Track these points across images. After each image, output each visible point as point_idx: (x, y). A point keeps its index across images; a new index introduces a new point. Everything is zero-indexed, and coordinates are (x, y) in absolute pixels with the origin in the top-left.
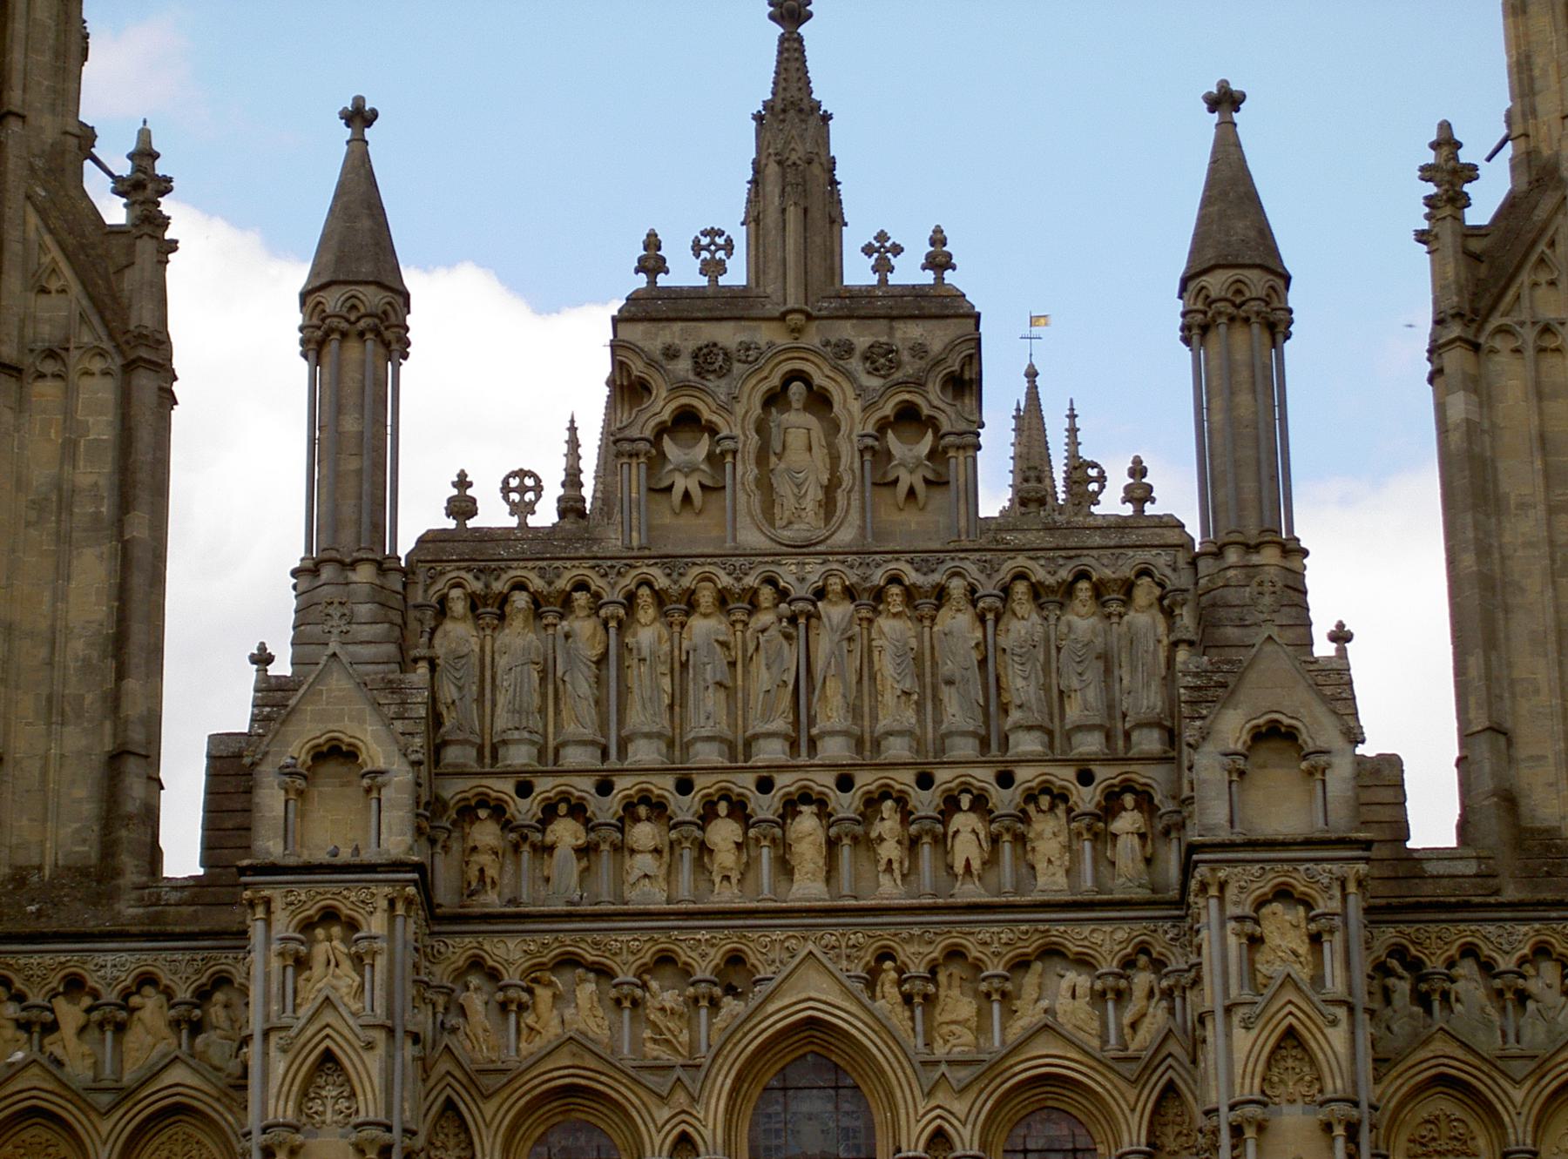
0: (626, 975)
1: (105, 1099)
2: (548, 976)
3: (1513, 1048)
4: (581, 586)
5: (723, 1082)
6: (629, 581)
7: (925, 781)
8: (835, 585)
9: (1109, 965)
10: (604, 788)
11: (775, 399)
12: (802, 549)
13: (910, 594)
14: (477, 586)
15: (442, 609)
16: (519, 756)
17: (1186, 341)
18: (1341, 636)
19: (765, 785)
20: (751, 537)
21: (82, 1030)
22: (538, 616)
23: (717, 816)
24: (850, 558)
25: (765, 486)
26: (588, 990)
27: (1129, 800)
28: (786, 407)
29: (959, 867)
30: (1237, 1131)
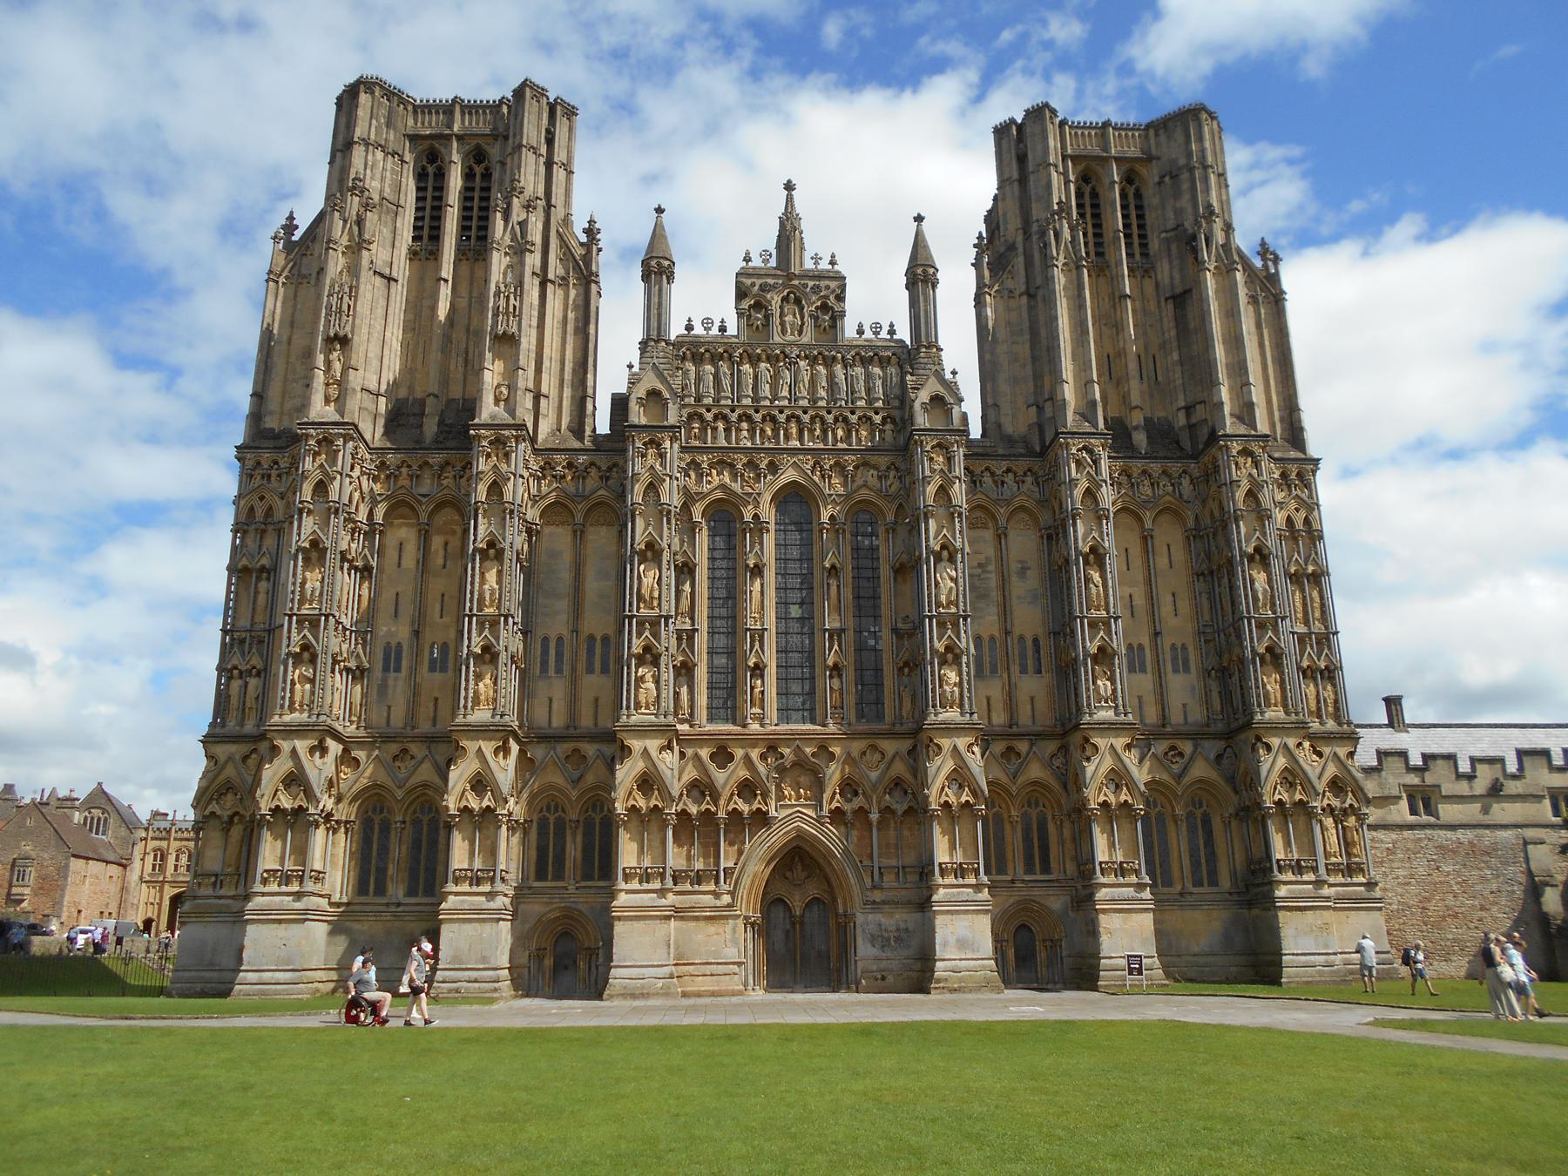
3: (1000, 497)
5: (767, 497)
9: (884, 468)
11: (785, 299)
13: (824, 358)
14: (694, 350)
16: (708, 401)
17: (907, 288)
18: (954, 373)
20: (777, 339)
25: (783, 324)
27: (889, 420)
28: (788, 302)
29: (839, 438)
30: (925, 514)
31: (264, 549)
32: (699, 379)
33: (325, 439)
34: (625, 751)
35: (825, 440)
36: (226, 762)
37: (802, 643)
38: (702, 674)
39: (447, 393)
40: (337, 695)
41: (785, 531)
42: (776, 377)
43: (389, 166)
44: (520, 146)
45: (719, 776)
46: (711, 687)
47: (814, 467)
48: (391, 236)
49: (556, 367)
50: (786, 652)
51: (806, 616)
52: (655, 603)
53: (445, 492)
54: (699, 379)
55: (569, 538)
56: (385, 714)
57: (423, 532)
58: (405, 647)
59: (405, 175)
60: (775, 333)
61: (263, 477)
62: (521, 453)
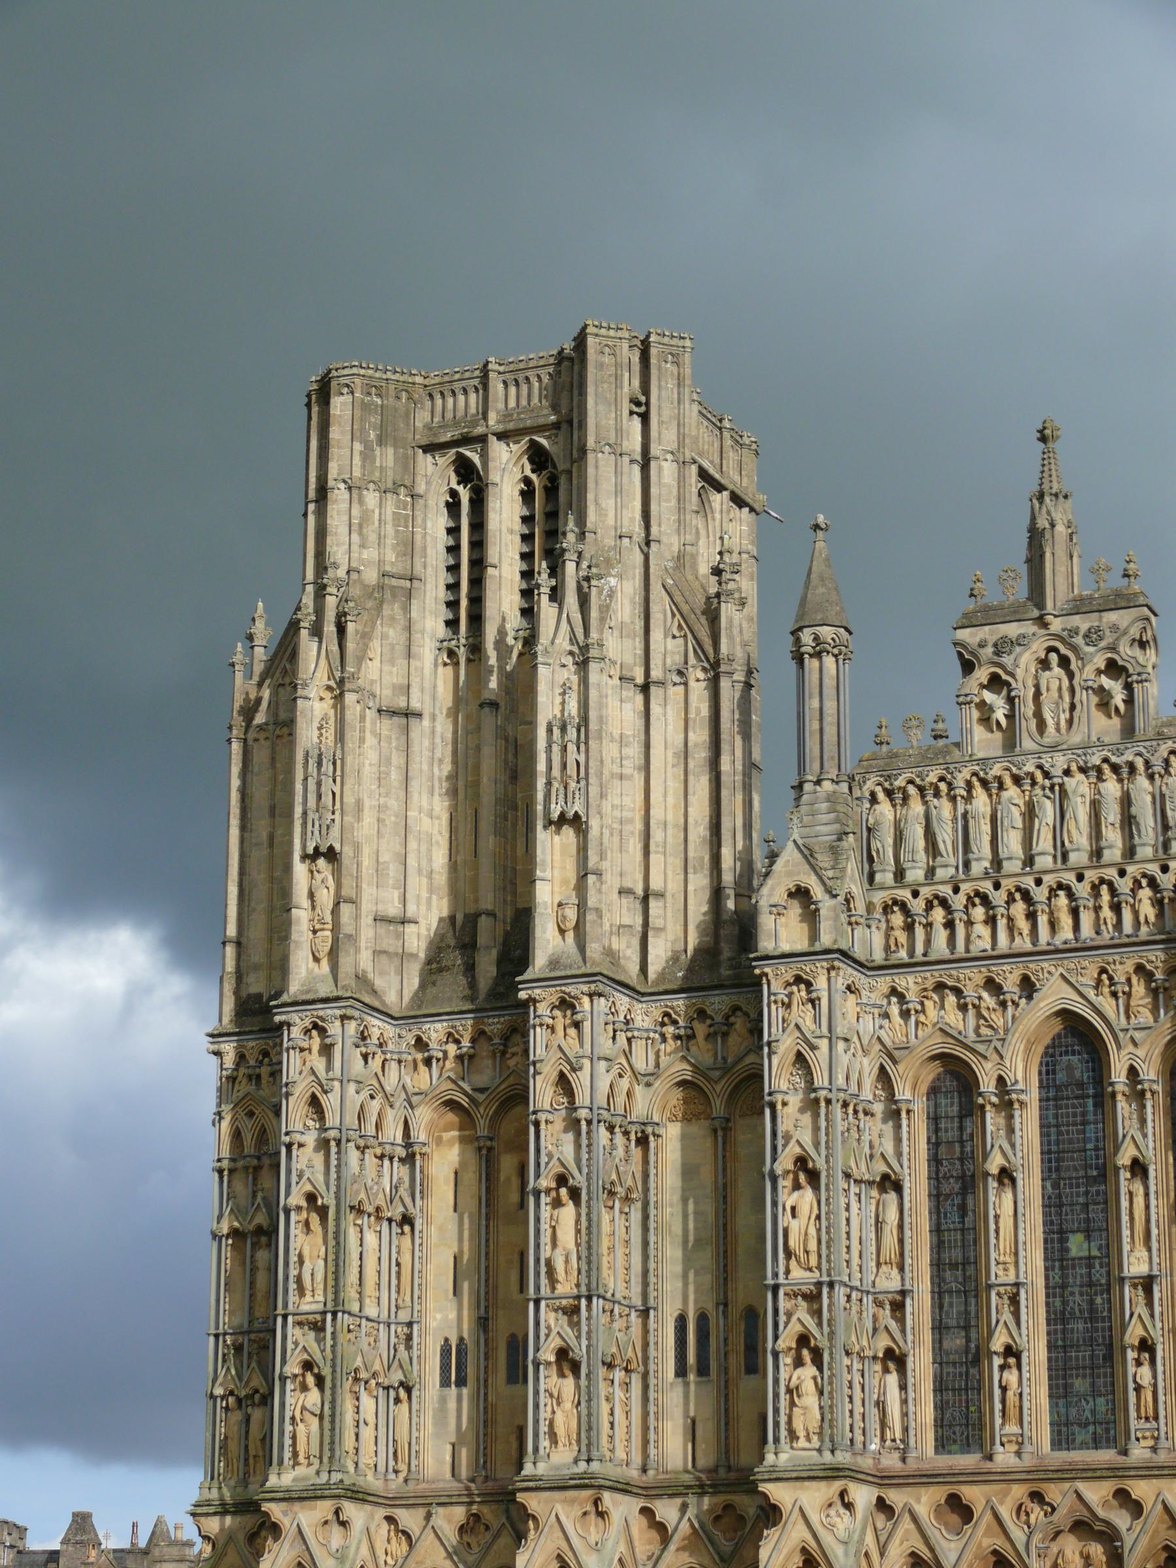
0: (969, 992)
1: (717, 1073)
2: (931, 994)
4: (942, 779)
6: (966, 774)
7: (1122, 873)
8: (1074, 767)
10: (956, 890)
12: (1054, 748)
13: (1115, 768)
15: (874, 799)
19: (1038, 882)
21: (708, 1037)
22: (923, 796)
23: (1014, 900)
24: (1079, 752)
25: (1038, 714)
26: (951, 999)
31: (259, 1200)
32: (899, 838)
33: (315, 1026)
34: (771, 1514)
35: (1118, 925)
36: (226, 1545)
37: (1091, 1302)
38: (922, 1364)
39: (514, 903)
40: (367, 1433)
41: (1055, 1099)
42: (1030, 813)
43: (390, 508)
44: (583, 451)
45: (949, 1548)
46: (940, 1387)
47: (1099, 982)
48: (403, 639)
49: (674, 837)
50: (1064, 1321)
51: (1095, 1253)
52: (813, 1262)
53: (511, 1080)
54: (899, 838)
55: (709, 1143)
56: (448, 1458)
57: (484, 1152)
58: (471, 1348)
59: (419, 520)
60: (1025, 735)
61: (250, 1077)
62: (600, 1021)
